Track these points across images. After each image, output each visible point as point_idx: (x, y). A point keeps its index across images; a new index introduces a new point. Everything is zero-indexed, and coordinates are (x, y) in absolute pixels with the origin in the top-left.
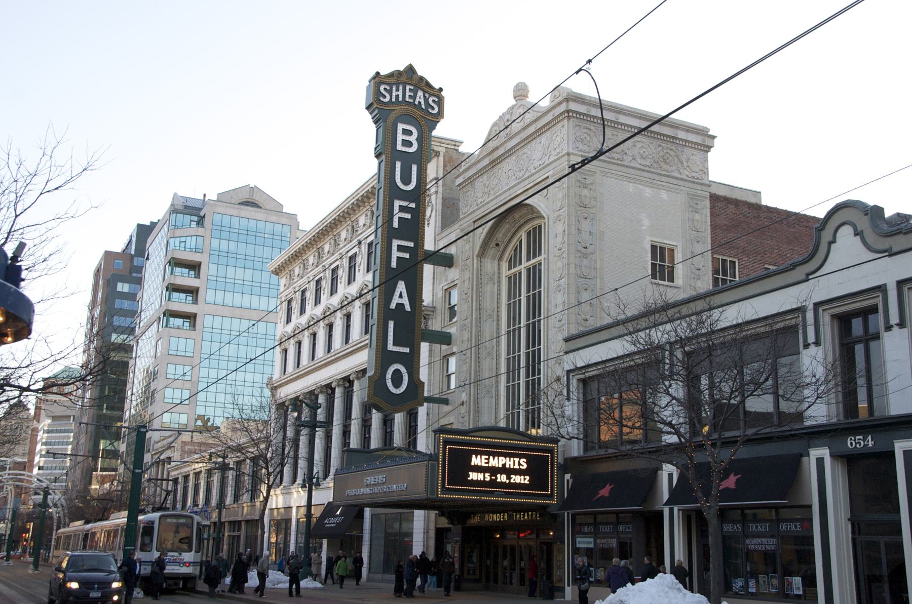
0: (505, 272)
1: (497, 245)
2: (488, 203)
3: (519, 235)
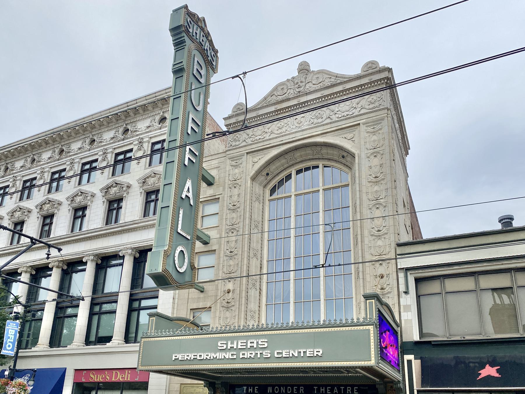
1: (268, 174)
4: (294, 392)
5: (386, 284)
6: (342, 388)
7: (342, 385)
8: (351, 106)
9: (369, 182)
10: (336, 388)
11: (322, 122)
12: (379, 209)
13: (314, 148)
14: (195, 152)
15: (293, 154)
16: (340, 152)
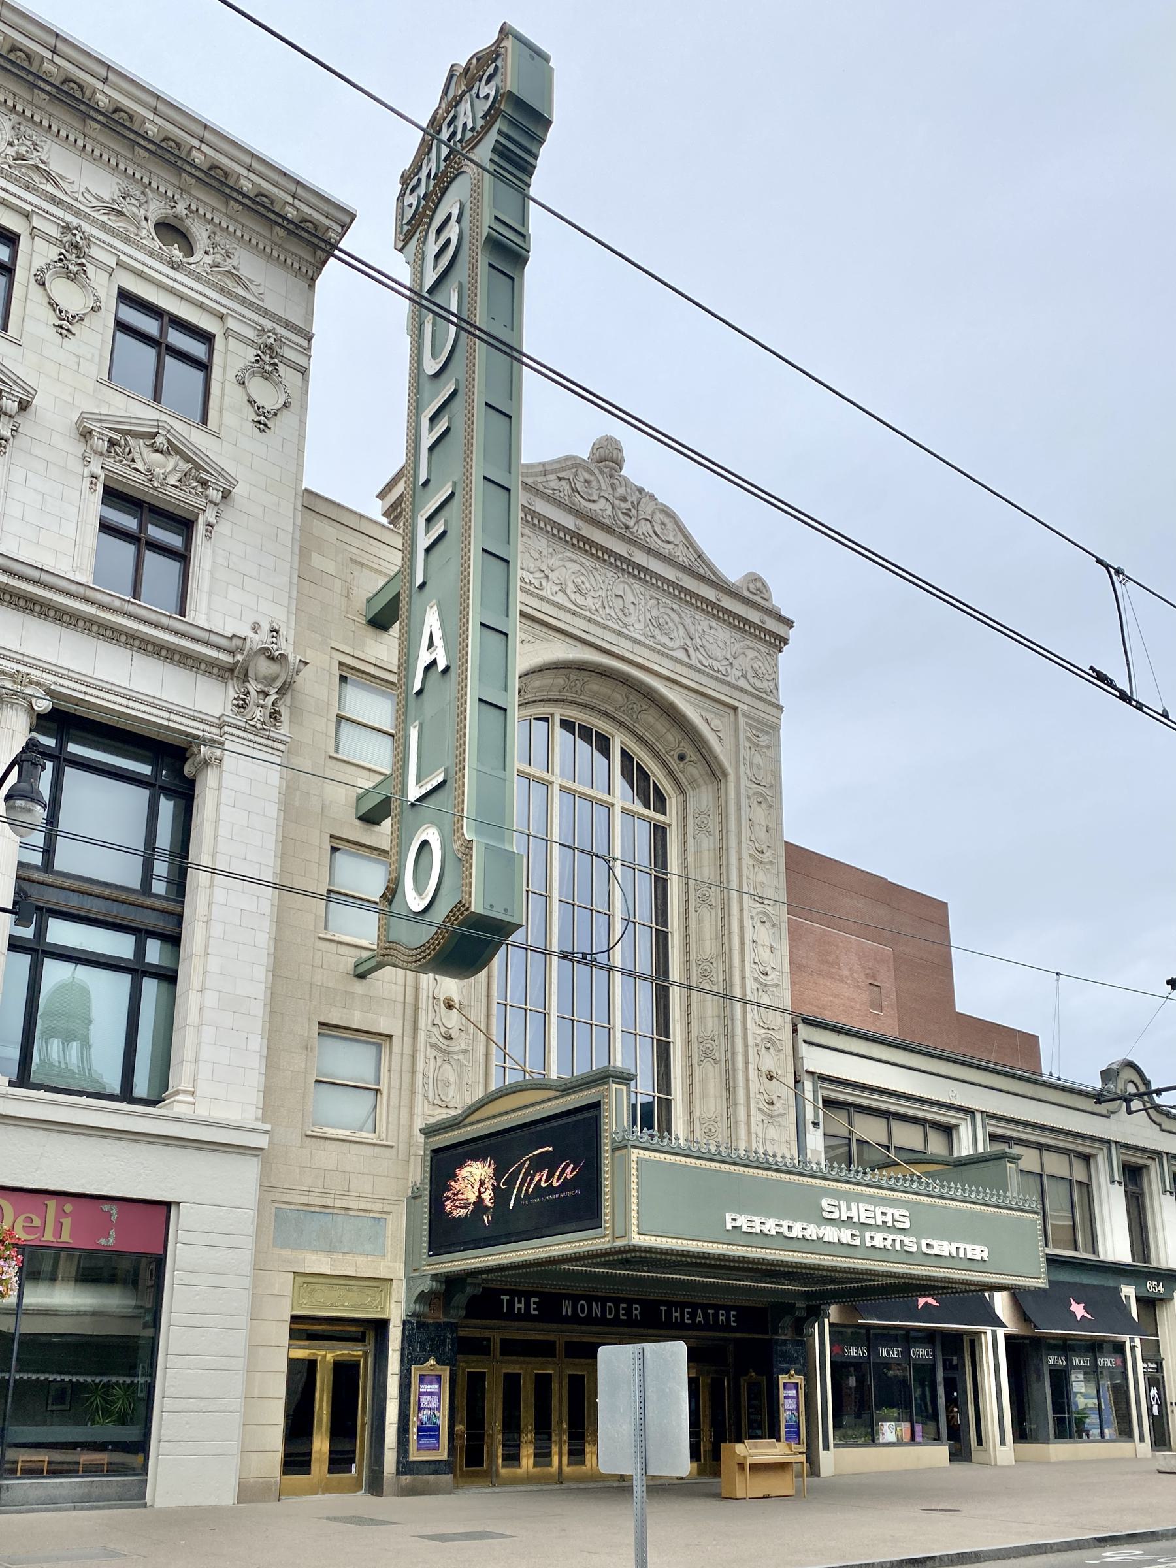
4: (533, 1312)
6: (711, 1311)
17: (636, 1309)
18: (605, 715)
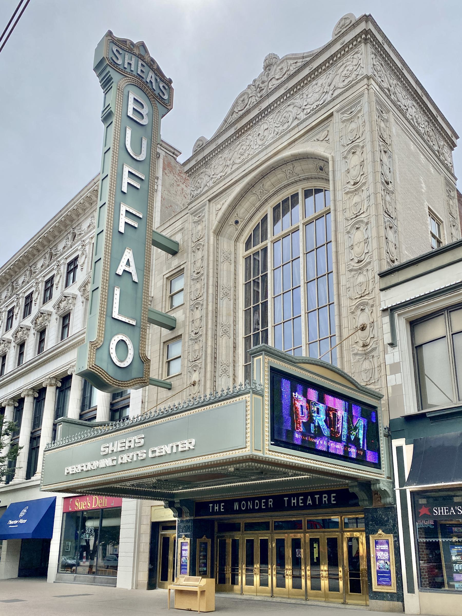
0: (242, 252)
2: (231, 174)
3: (265, 210)
5: (369, 338)
7: (317, 493)
8: (321, 92)
9: (347, 193)
10: (309, 497)
11: (289, 127)
12: (360, 229)
13: (285, 168)
14: (138, 215)
15: (261, 186)
16: (316, 163)
17: (325, 497)
18: (285, 187)
